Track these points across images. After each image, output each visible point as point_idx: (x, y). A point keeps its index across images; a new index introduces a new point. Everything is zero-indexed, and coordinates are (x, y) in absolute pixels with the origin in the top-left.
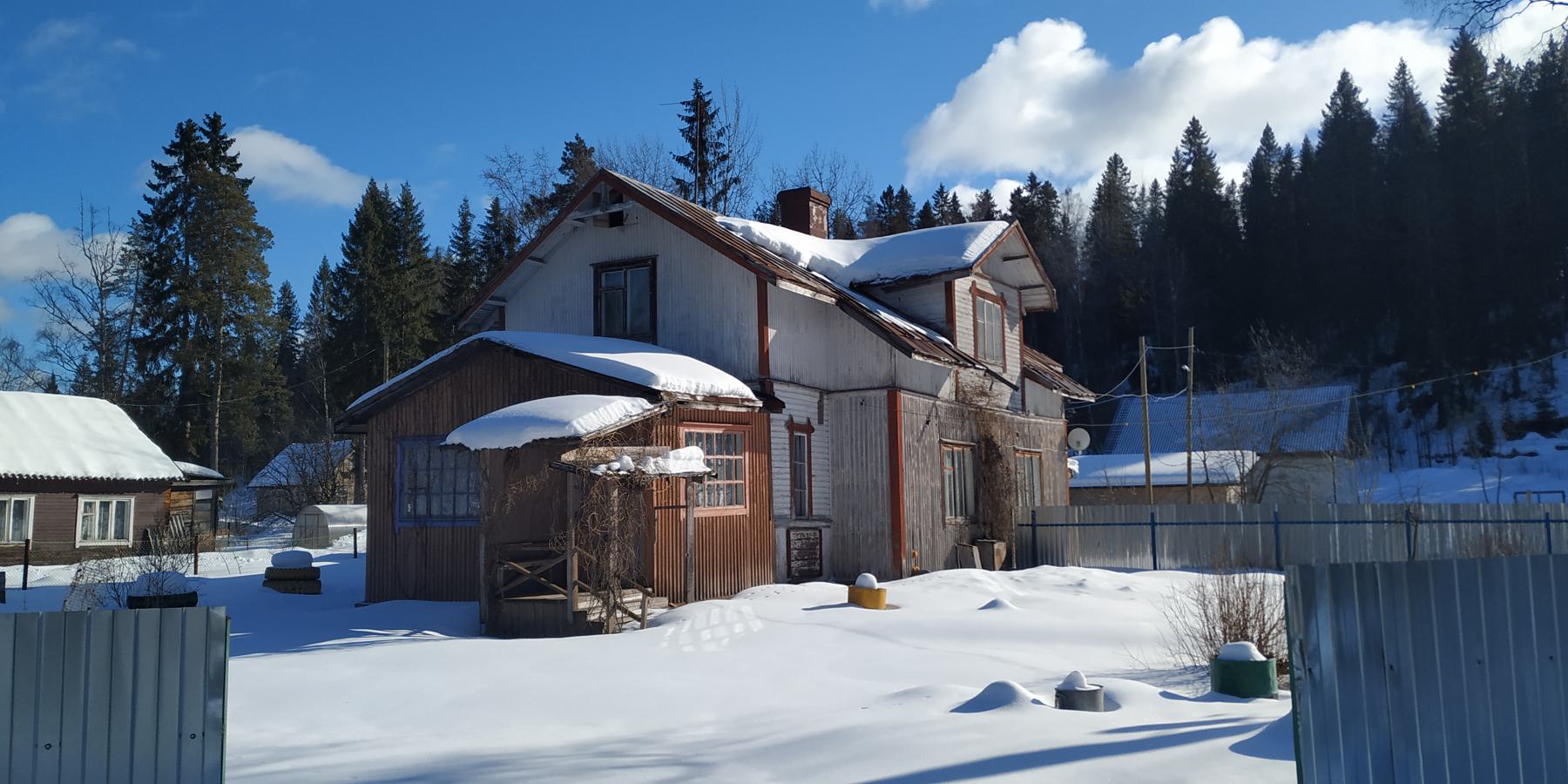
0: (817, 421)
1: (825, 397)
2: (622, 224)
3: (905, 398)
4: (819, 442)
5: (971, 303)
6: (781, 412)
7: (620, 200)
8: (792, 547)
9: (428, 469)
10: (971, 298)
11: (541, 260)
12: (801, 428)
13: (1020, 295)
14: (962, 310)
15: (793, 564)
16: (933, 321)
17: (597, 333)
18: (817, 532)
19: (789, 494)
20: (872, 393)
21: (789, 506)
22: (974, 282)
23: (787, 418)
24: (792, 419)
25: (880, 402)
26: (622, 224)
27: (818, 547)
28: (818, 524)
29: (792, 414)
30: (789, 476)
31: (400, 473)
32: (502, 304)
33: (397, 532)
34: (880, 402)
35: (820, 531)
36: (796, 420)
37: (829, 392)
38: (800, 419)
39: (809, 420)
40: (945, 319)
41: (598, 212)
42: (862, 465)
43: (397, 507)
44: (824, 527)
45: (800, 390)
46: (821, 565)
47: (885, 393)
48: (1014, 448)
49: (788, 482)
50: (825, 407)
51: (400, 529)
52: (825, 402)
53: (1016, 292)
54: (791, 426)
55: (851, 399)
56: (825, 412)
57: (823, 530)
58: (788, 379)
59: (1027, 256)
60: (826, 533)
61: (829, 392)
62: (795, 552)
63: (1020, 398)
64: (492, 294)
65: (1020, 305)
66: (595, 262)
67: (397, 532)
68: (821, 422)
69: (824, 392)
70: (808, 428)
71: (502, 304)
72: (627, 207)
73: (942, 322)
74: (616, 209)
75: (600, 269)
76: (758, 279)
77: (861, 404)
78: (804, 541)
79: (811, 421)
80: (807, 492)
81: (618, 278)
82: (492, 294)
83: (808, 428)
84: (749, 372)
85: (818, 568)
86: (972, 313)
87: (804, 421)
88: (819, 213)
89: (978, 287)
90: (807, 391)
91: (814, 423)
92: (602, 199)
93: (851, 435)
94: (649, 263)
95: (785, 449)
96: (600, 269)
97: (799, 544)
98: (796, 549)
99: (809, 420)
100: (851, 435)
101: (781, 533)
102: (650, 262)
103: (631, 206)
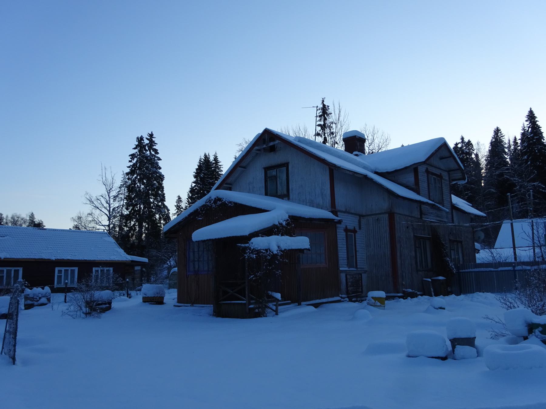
0: (358, 228)
1: (362, 218)
2: (275, 151)
3: (397, 217)
4: (360, 238)
5: (426, 177)
6: (341, 224)
7: (274, 140)
8: (348, 281)
9: (199, 251)
10: (426, 175)
11: (244, 168)
12: (351, 231)
13: (449, 174)
14: (422, 180)
15: (349, 288)
16: (409, 185)
17: (266, 194)
18: (360, 276)
19: (346, 258)
20: (382, 215)
21: (346, 264)
22: (427, 168)
23: (344, 226)
24: (346, 227)
25: (385, 218)
26: (275, 151)
27: (360, 281)
28: (360, 272)
29: (347, 224)
31: (189, 252)
32: (230, 186)
33: (188, 276)
34: (385, 218)
35: (361, 275)
36: (348, 227)
37: (363, 216)
38: (350, 227)
39: (354, 228)
40: (414, 184)
41: (265, 146)
42: (379, 246)
43: (188, 267)
44: (363, 273)
45: (350, 215)
46: (362, 289)
47: (387, 216)
48: (449, 239)
49: (346, 254)
50: (362, 222)
51: (189, 275)
52: (362, 220)
53: (447, 173)
54: (346, 230)
55: (373, 219)
56: (362, 224)
57: (363, 274)
58: (344, 210)
59: (450, 157)
60: (364, 276)
61: (363, 216)
62: (350, 284)
63: (451, 218)
64: (226, 182)
65: (449, 178)
66: (265, 167)
67: (188, 276)
68: (360, 228)
69: (361, 216)
70: (354, 231)
71: (230, 186)
72: (276, 143)
73: (413, 185)
74: (271, 144)
75: (267, 169)
76: (330, 168)
77: (377, 220)
78: (354, 279)
79: (356, 227)
80: (355, 257)
81: (274, 172)
82: (226, 182)
83: (354, 231)
84: (327, 207)
85: (361, 290)
86: (426, 181)
89: (429, 170)
91: (357, 229)
92: (266, 140)
93: (374, 233)
94: (286, 165)
95: (343, 239)
96: (267, 169)
97: (351, 280)
98: (350, 282)
99: (354, 228)
100: (374, 233)
101: (343, 276)
102: (286, 165)
103: (277, 142)
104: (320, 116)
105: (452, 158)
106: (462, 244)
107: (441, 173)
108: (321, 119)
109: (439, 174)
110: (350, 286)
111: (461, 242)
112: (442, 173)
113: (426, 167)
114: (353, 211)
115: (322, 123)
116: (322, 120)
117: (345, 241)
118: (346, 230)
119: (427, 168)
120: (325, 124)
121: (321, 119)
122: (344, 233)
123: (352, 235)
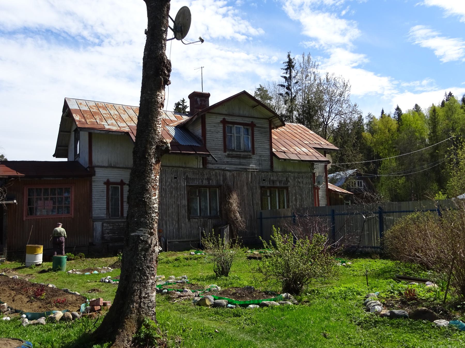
19: (105, 208)
21: (105, 213)
30: (106, 202)
32: (66, 148)
54: (108, 183)
58: (106, 164)
80: (120, 208)
87: (119, 181)
88: (201, 101)
89: (227, 120)
90: (122, 170)
104: (286, 69)
105: (260, 106)
106: (287, 190)
107: (252, 122)
108: (287, 73)
109: (250, 123)
110: (108, 233)
111: (287, 188)
112: (254, 121)
113: (223, 117)
114: (121, 166)
115: (288, 76)
116: (288, 72)
117: (105, 193)
118: (108, 183)
119: (224, 119)
120: (290, 77)
121: (287, 73)
122: (105, 186)
123: (119, 188)
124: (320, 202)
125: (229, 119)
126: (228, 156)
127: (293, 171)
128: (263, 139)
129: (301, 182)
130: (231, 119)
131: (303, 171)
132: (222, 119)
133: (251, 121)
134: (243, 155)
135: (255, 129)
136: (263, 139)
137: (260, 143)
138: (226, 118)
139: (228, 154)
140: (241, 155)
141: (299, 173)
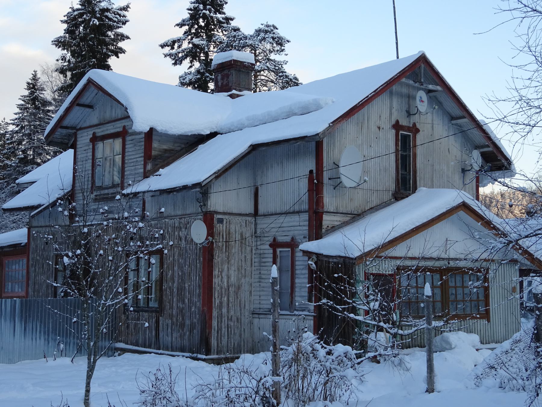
109: (121, 129)
113: (92, 132)
124: (297, 281)
125: (100, 132)
126: (96, 199)
127: (173, 214)
128: (137, 156)
129: (183, 239)
130: (102, 131)
131: (188, 212)
132: (91, 136)
133: (123, 125)
134: (112, 194)
135: (128, 138)
136: (137, 156)
137: (132, 164)
138: (96, 131)
139: (96, 196)
140: (108, 194)
141: (181, 217)
